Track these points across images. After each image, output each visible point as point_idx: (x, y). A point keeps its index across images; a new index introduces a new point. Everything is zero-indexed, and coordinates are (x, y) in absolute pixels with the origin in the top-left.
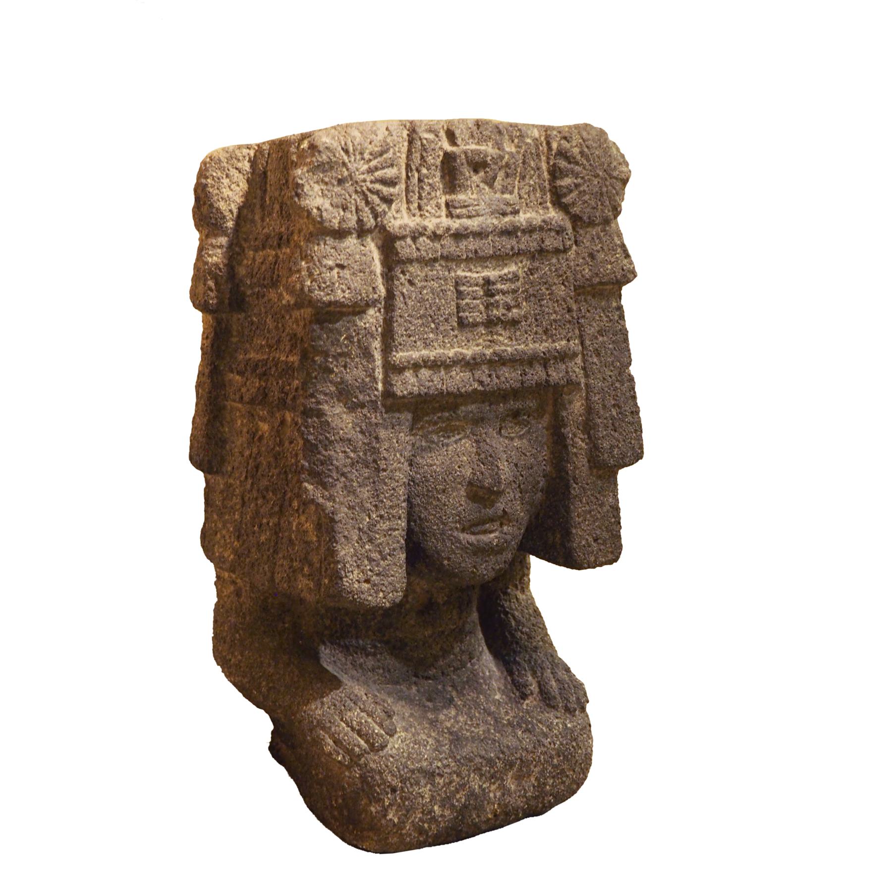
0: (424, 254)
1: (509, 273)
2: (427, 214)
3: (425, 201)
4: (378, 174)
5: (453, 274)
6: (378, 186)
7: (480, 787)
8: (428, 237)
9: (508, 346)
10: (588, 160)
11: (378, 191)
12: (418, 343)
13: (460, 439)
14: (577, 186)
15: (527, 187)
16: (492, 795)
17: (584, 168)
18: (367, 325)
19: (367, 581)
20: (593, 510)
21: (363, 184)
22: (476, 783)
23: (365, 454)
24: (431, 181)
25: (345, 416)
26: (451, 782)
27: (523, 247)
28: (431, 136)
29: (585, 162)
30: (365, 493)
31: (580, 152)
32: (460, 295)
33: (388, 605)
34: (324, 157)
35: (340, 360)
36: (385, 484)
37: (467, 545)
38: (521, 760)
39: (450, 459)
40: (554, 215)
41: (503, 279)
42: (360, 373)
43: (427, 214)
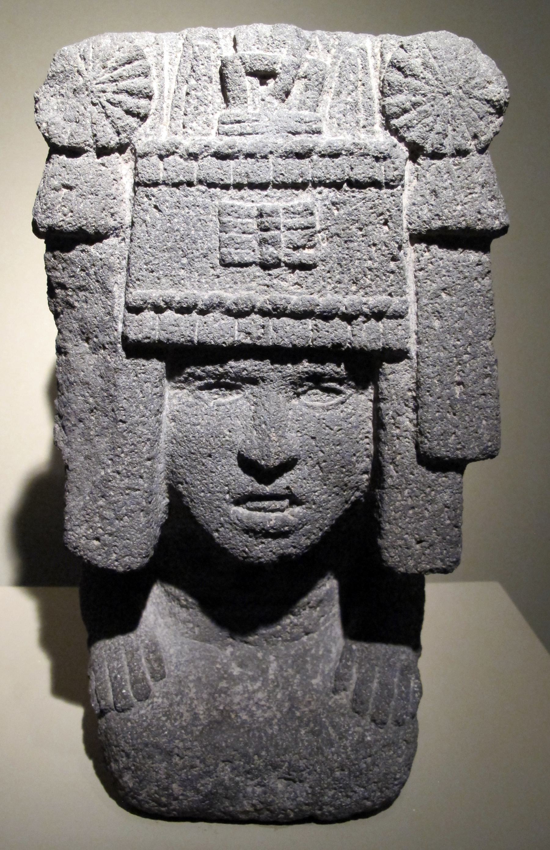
0: (173, 175)
1: (299, 205)
2: (190, 131)
3: (190, 116)
4: (122, 84)
5: (217, 202)
6: (123, 97)
7: (231, 779)
8: (181, 157)
9: (294, 293)
10: (434, 74)
11: (120, 102)
12: (163, 280)
13: (237, 400)
14: (415, 105)
15: (342, 105)
16: (249, 789)
17: (427, 83)
18: (104, 256)
19: (98, 539)
20: (418, 506)
21: (101, 94)
22: (225, 773)
23: (103, 401)
24: (199, 94)
25: (87, 357)
26: (192, 767)
27: (319, 174)
28: (208, 43)
29: (429, 76)
30: (103, 444)
31: (423, 64)
32: (224, 227)
33: (121, 569)
34: (59, 66)
35: (81, 294)
36: (125, 438)
37: (237, 522)
38: (289, 763)
39: (219, 420)
40: (381, 139)
41: (287, 211)
42: (99, 310)
43: (190, 131)
